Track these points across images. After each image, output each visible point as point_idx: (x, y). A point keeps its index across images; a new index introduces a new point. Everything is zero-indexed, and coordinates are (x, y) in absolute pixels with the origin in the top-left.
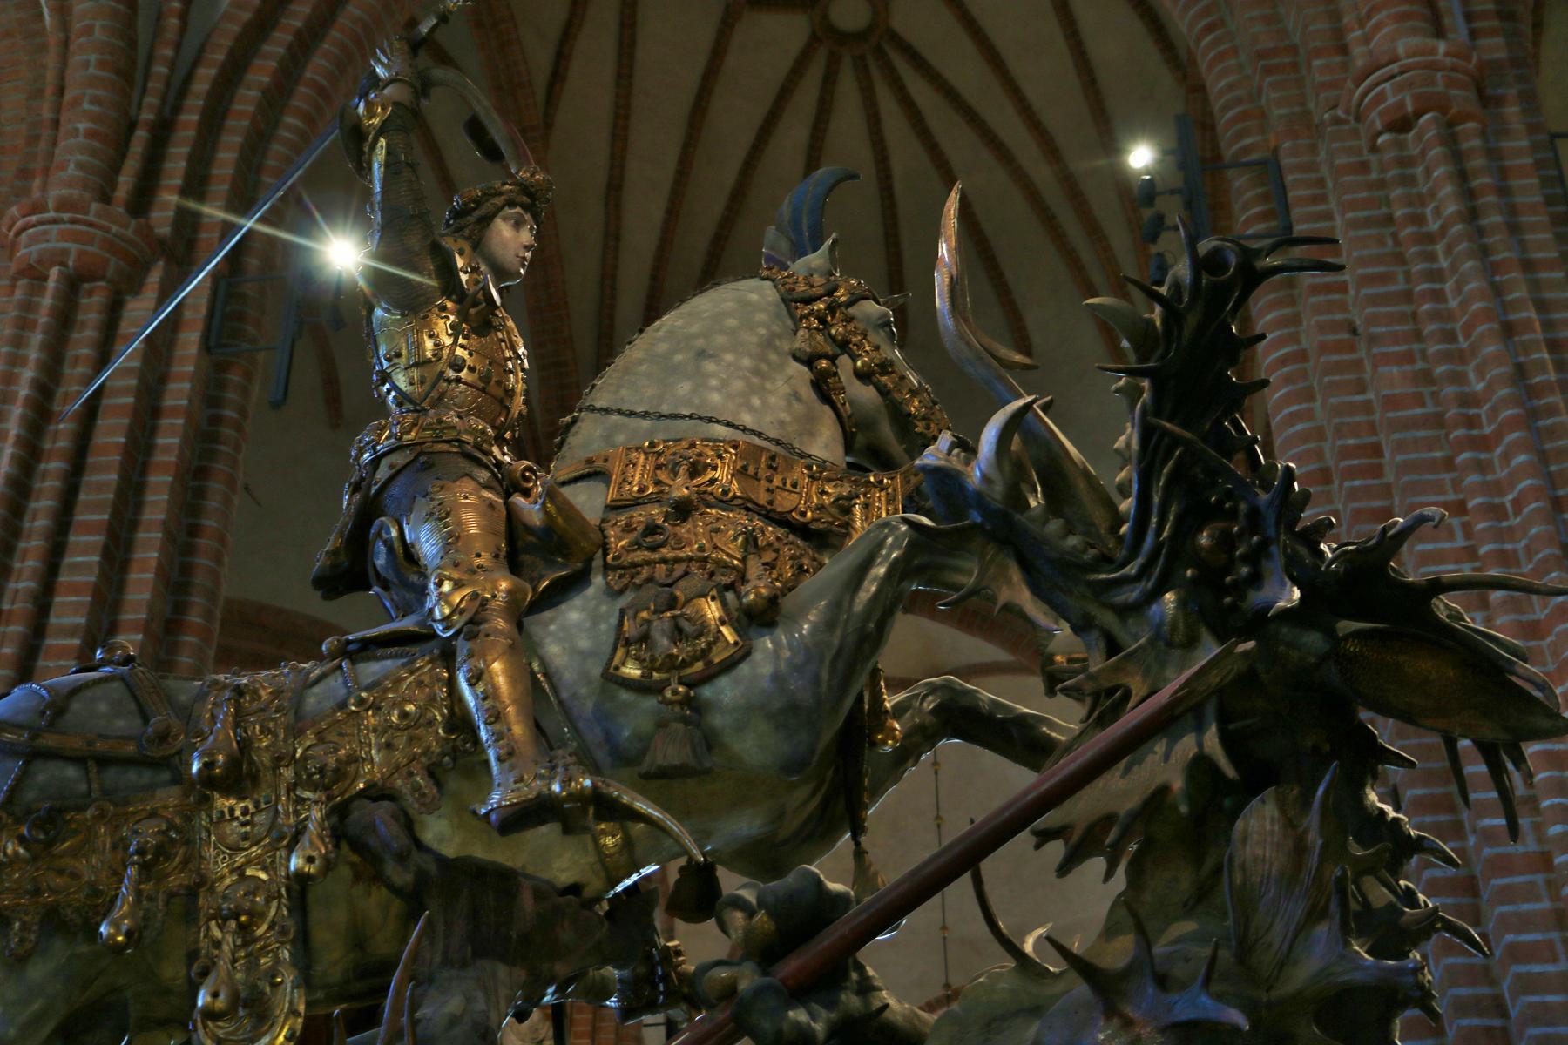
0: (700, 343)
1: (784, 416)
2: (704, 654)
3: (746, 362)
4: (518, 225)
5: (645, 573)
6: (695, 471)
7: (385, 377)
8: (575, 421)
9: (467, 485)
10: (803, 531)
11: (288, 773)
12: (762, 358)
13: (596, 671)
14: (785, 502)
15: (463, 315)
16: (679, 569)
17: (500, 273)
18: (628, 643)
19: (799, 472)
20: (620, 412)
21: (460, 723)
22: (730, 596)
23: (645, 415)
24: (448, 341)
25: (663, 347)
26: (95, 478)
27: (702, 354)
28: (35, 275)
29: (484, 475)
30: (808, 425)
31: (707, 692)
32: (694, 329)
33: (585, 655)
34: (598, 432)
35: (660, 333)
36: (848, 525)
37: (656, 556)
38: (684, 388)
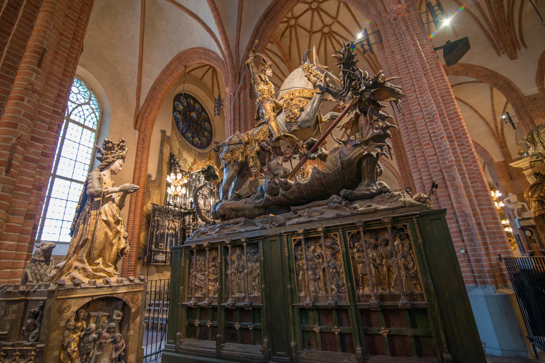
3: (298, 79)
4: (269, 70)
6: (293, 94)
9: (267, 104)
10: (308, 98)
12: (300, 78)
14: (305, 95)
15: (264, 83)
17: (269, 77)
19: (307, 91)
21: (270, 131)
22: (298, 109)
27: (293, 80)
29: (269, 102)
30: (308, 84)
31: (297, 121)
33: (283, 120)
38: (291, 84)
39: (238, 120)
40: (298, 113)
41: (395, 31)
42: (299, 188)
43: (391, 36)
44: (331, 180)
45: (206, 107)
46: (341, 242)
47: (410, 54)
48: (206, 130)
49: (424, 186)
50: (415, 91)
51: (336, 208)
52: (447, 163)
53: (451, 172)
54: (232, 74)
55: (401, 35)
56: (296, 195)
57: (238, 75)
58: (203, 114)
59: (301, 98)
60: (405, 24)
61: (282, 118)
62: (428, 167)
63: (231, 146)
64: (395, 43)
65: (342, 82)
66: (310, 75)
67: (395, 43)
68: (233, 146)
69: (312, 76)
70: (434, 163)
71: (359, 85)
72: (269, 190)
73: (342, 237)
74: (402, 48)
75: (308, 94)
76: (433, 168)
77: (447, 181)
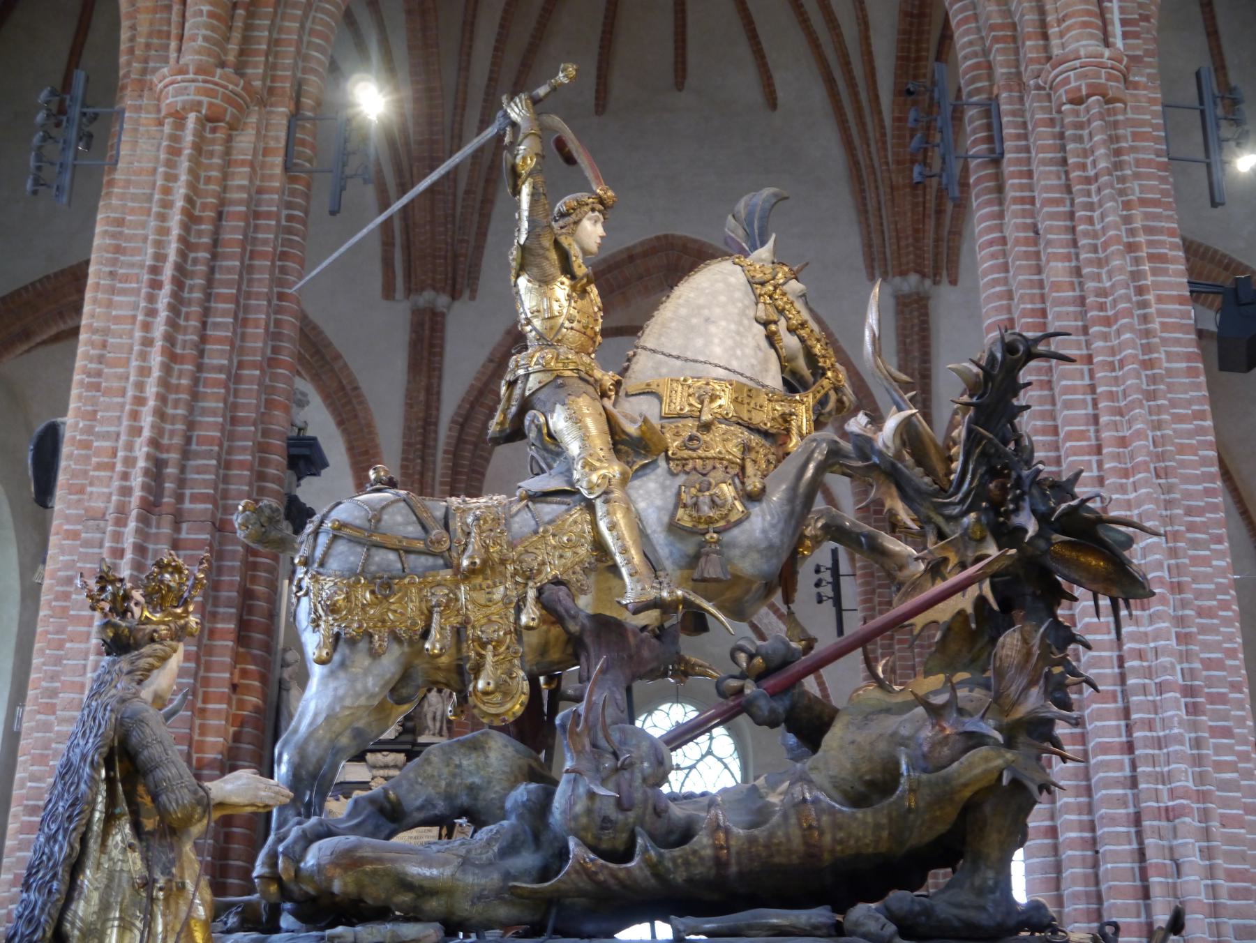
0: (706, 312)
1: (754, 361)
2: (725, 517)
5: (690, 466)
7: (529, 322)
8: (635, 355)
10: (765, 434)
11: (510, 568)
12: (740, 323)
13: (666, 519)
15: (573, 288)
16: (709, 464)
18: (685, 506)
19: (763, 399)
20: (663, 354)
21: (599, 546)
23: (678, 358)
24: (565, 304)
26: (225, 263)
27: (707, 320)
28: (179, 118)
31: (726, 537)
32: (702, 301)
34: (650, 364)
35: (681, 301)
36: (788, 431)
37: (694, 455)
38: (699, 342)
40: (737, 503)
41: (1063, 148)
42: (722, 847)
43: (1043, 162)
44: (852, 842)
47: (1108, 284)
49: (1058, 868)
50: (1098, 450)
52: (1165, 795)
53: (1171, 836)
55: (1088, 181)
56: (699, 870)
60: (1114, 139)
62: (1089, 791)
64: (1057, 202)
65: (957, 465)
66: (775, 323)
67: (1057, 202)
68: (392, 556)
69: (783, 323)
70: (1116, 783)
71: (1018, 500)
74: (1083, 242)
75: (765, 416)
76: (1109, 801)
77: (1150, 871)
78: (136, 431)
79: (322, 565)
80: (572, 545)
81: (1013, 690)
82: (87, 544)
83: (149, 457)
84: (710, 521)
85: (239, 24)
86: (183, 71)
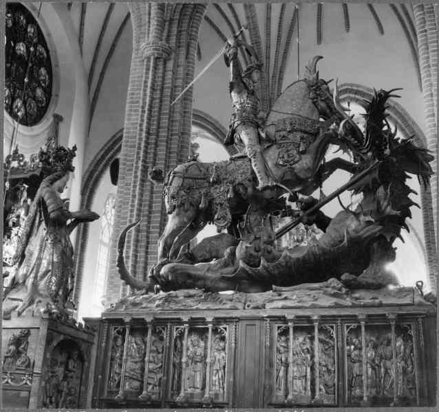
2: (293, 160)
7: (234, 106)
21: (253, 172)
24: (245, 99)
25: (284, 98)
28: (149, 58)
31: (294, 166)
39: (156, 109)
45: (49, 35)
46: (337, 335)
48: (40, 86)
51: (334, 295)
54: (158, 21)
57: (167, 23)
58: (40, 48)
59: (303, 134)
61: (273, 155)
63: (186, 181)
65: (365, 137)
66: (317, 98)
68: (191, 180)
72: (246, 258)
73: (340, 330)
78: (138, 158)
79: (170, 185)
80: (244, 173)
81: (383, 208)
82: (126, 194)
83: (142, 166)
84: (287, 162)
85: (167, 27)
86: (148, 44)
